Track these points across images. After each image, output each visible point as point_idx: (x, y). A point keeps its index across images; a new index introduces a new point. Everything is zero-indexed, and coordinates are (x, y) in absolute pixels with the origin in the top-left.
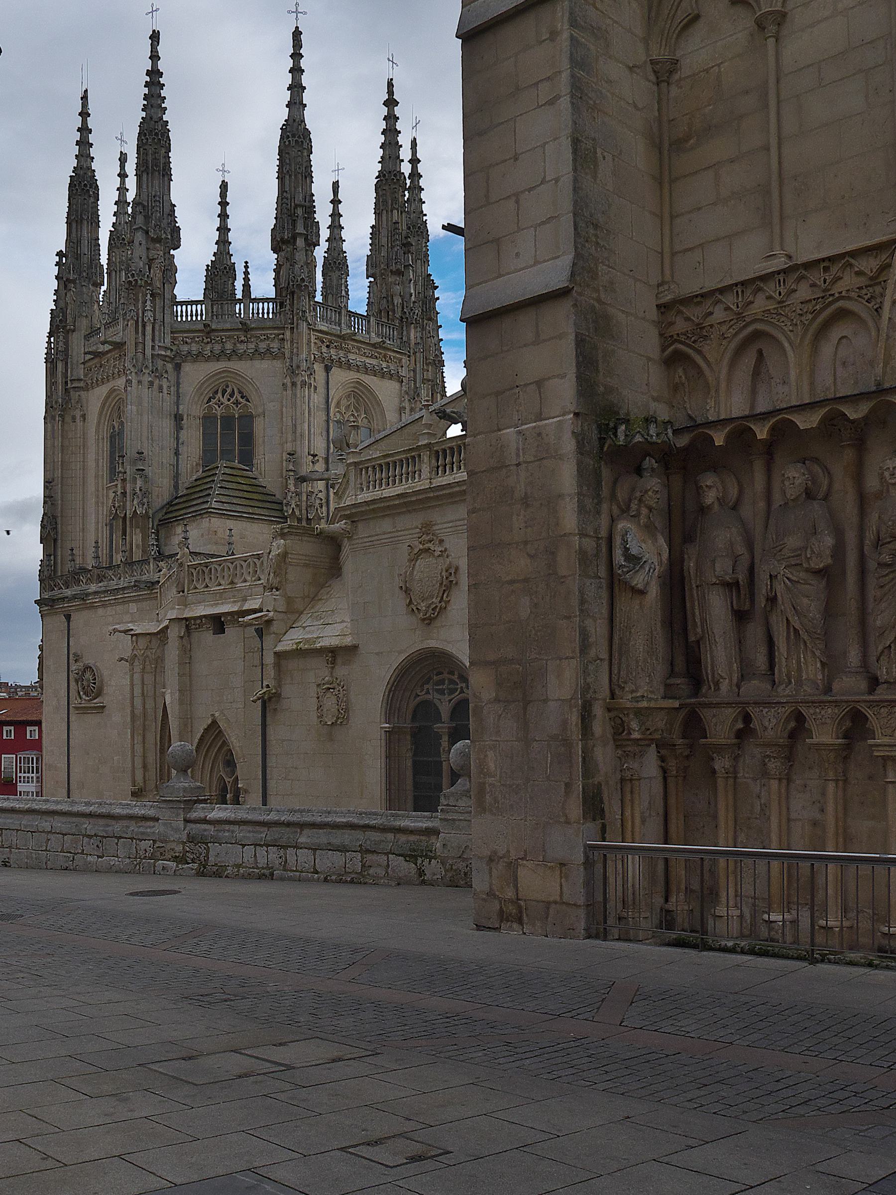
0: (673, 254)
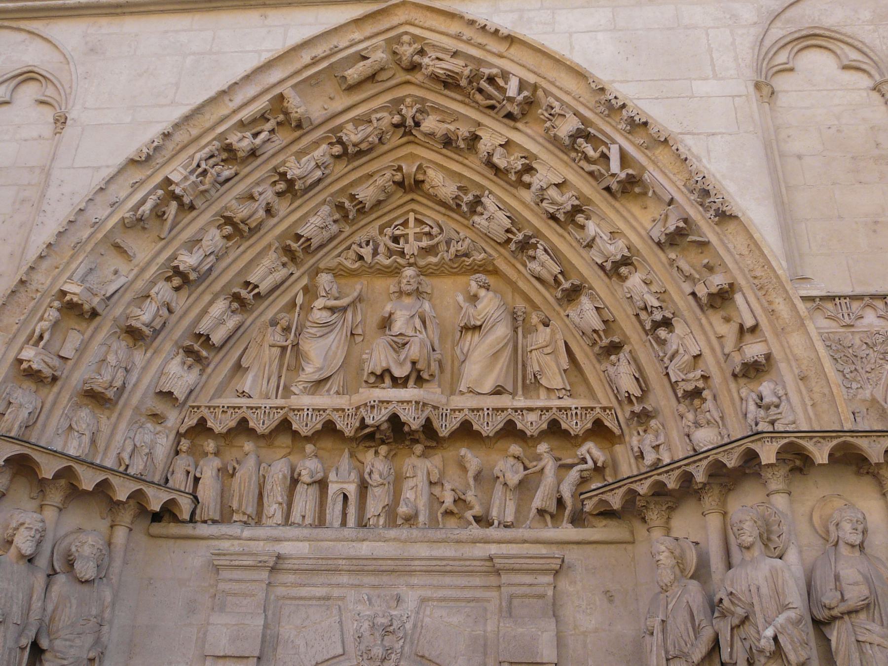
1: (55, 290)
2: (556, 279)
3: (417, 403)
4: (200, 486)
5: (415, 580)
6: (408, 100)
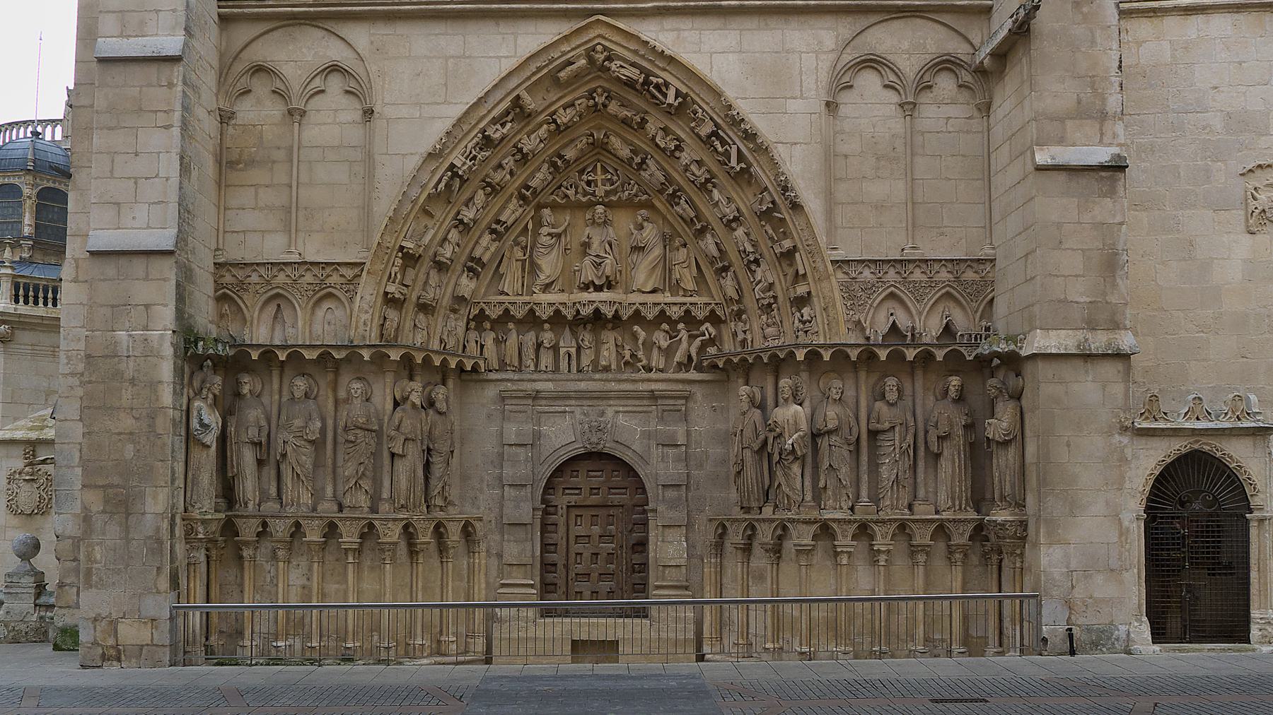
0: (225, 232)
1: (397, 247)
2: (692, 219)
3: (610, 302)
4: (485, 349)
5: (612, 402)
6: (599, 90)
